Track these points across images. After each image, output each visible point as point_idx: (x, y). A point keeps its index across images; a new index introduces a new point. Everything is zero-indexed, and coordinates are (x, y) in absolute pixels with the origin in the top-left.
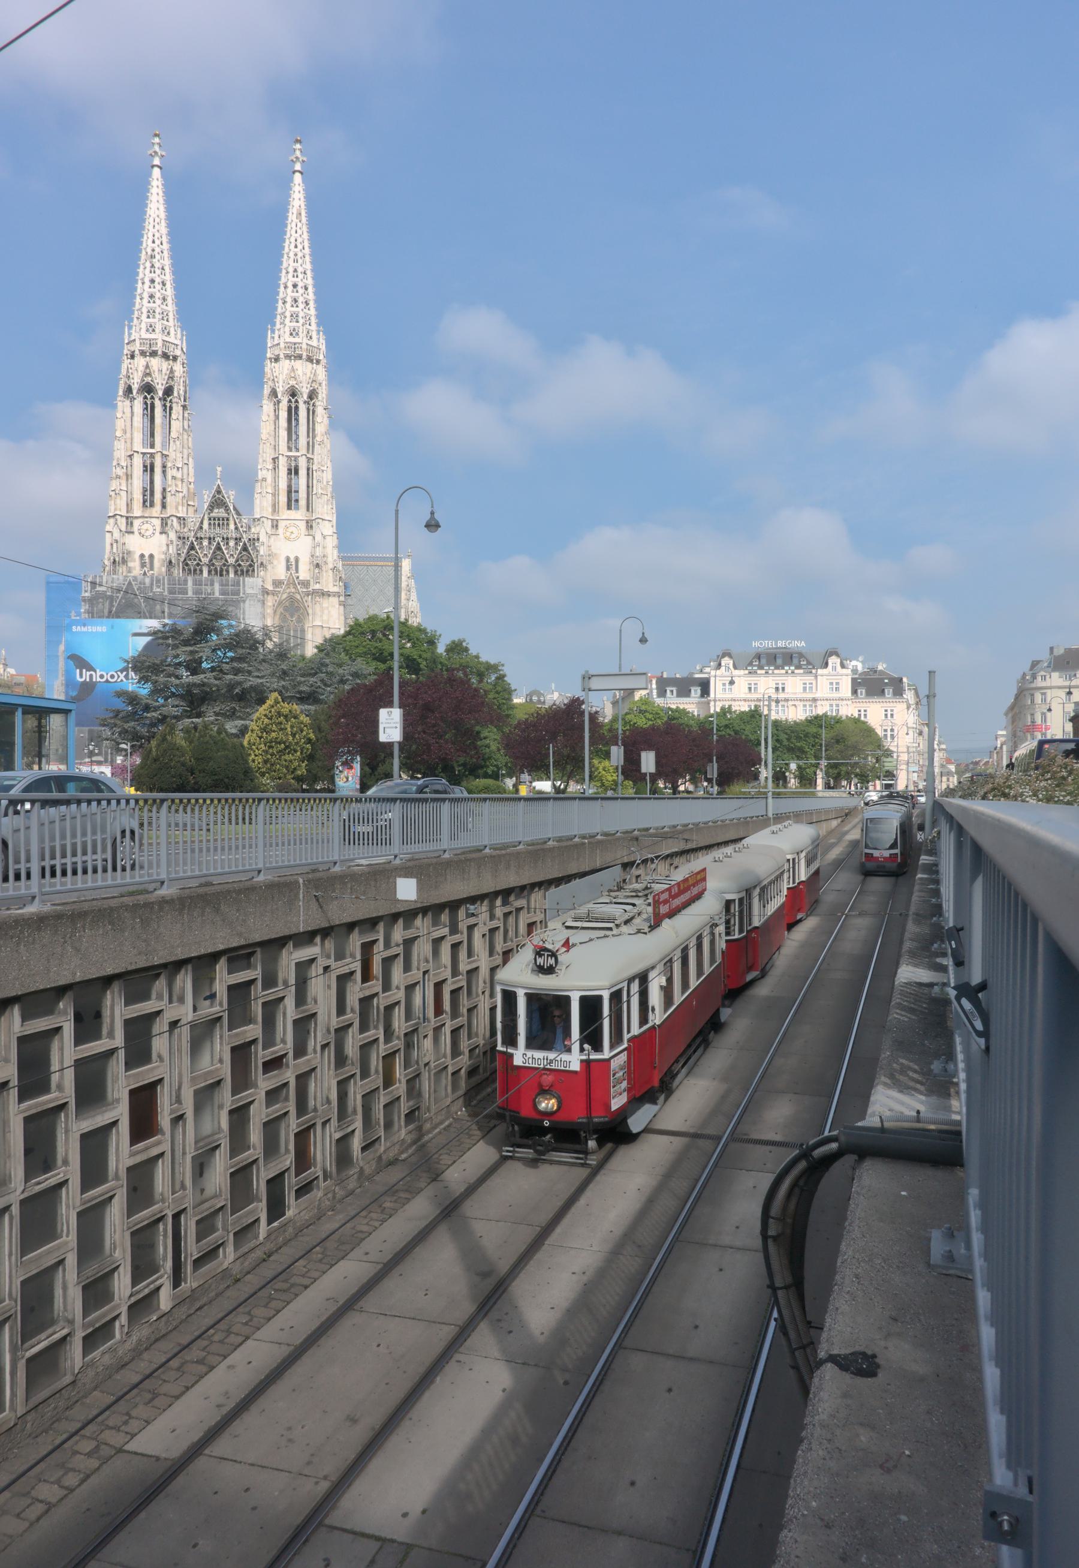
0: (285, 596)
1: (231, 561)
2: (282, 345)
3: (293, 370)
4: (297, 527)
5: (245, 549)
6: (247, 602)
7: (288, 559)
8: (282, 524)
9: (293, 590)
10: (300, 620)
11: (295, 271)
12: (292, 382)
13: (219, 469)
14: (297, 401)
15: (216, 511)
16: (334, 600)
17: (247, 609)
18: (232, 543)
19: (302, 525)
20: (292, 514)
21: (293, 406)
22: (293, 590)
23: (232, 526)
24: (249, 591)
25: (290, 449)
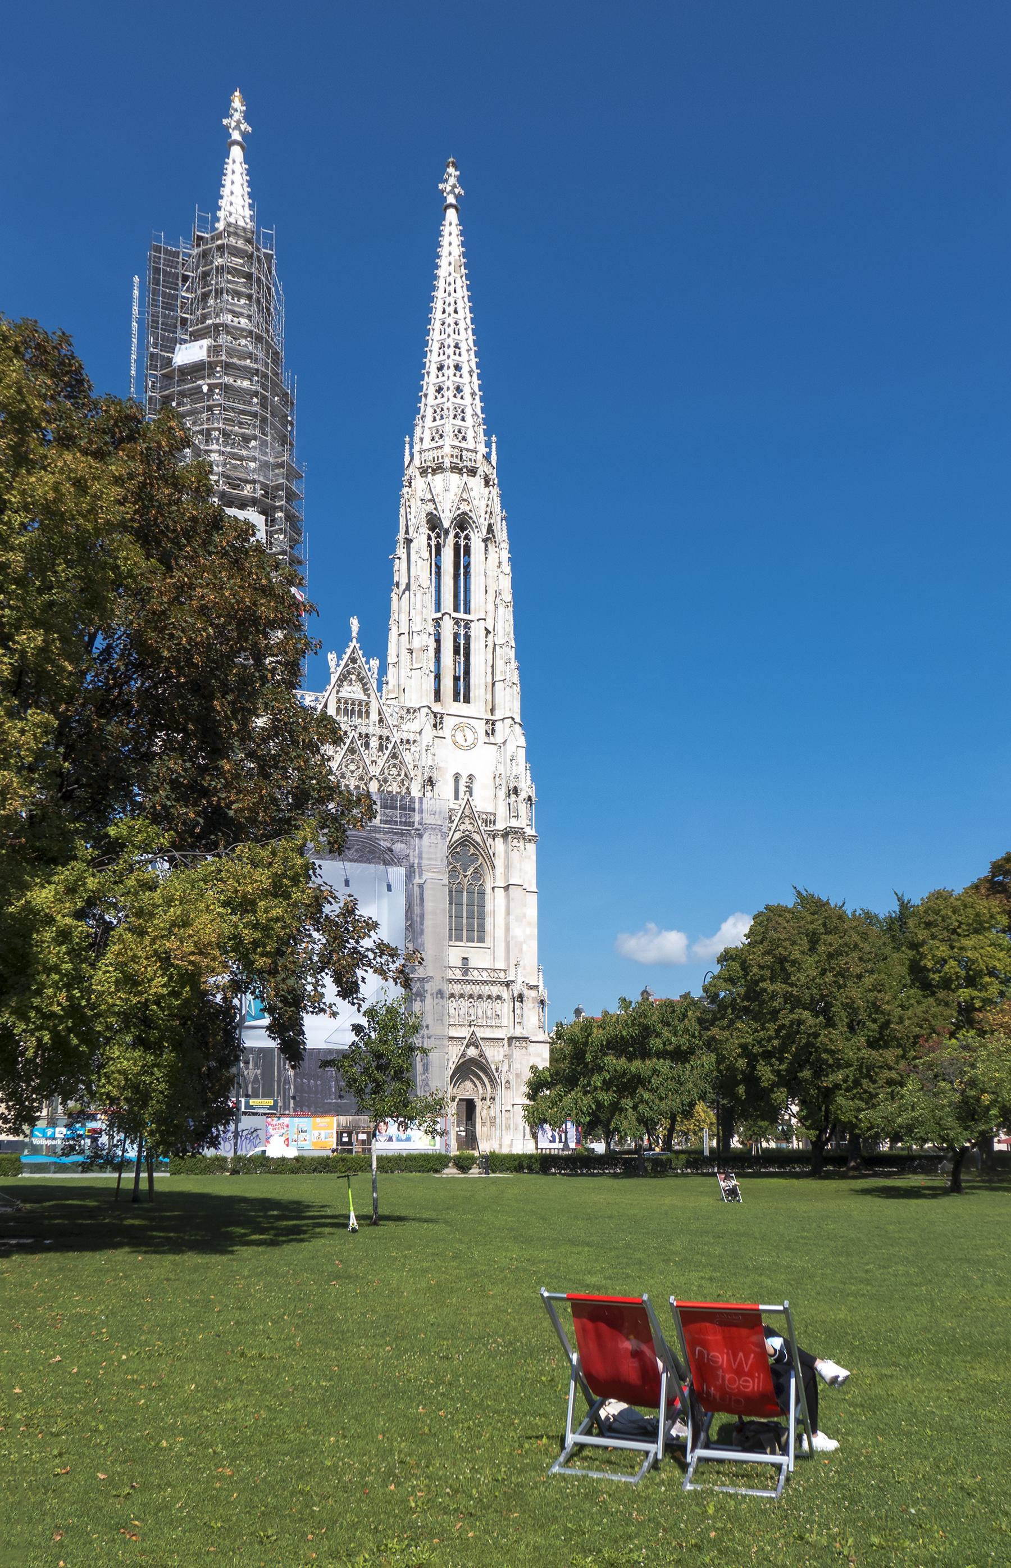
0: (458, 835)
1: (374, 770)
2: (447, 450)
3: (465, 488)
4: (472, 728)
5: (394, 756)
6: (426, 836)
7: (457, 777)
8: (449, 722)
9: (470, 827)
10: (478, 874)
11: (457, 346)
12: (464, 507)
13: (355, 624)
14: (467, 537)
15: (349, 689)
16: (531, 847)
17: (425, 850)
18: (374, 743)
19: (481, 727)
20: (460, 708)
21: (462, 543)
22: (470, 827)
23: (374, 717)
24: (428, 819)
25: (456, 609)
